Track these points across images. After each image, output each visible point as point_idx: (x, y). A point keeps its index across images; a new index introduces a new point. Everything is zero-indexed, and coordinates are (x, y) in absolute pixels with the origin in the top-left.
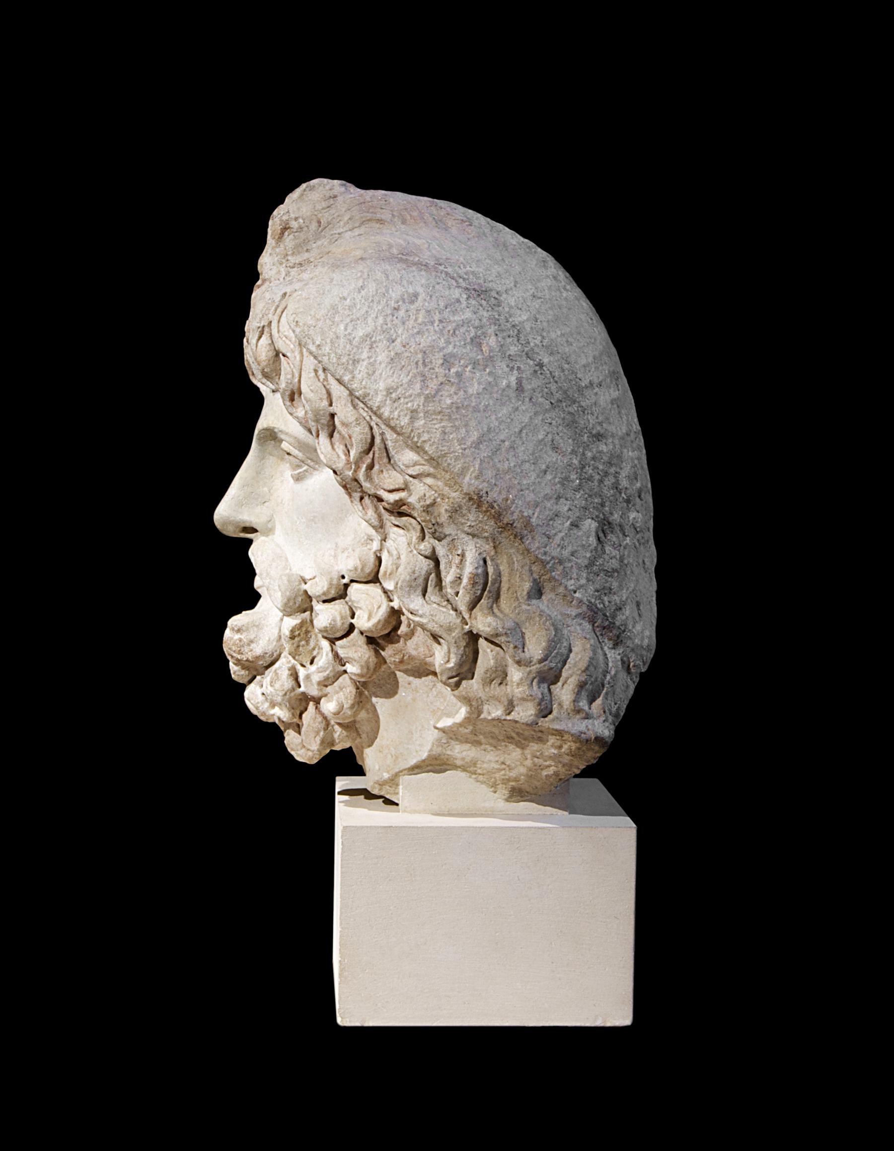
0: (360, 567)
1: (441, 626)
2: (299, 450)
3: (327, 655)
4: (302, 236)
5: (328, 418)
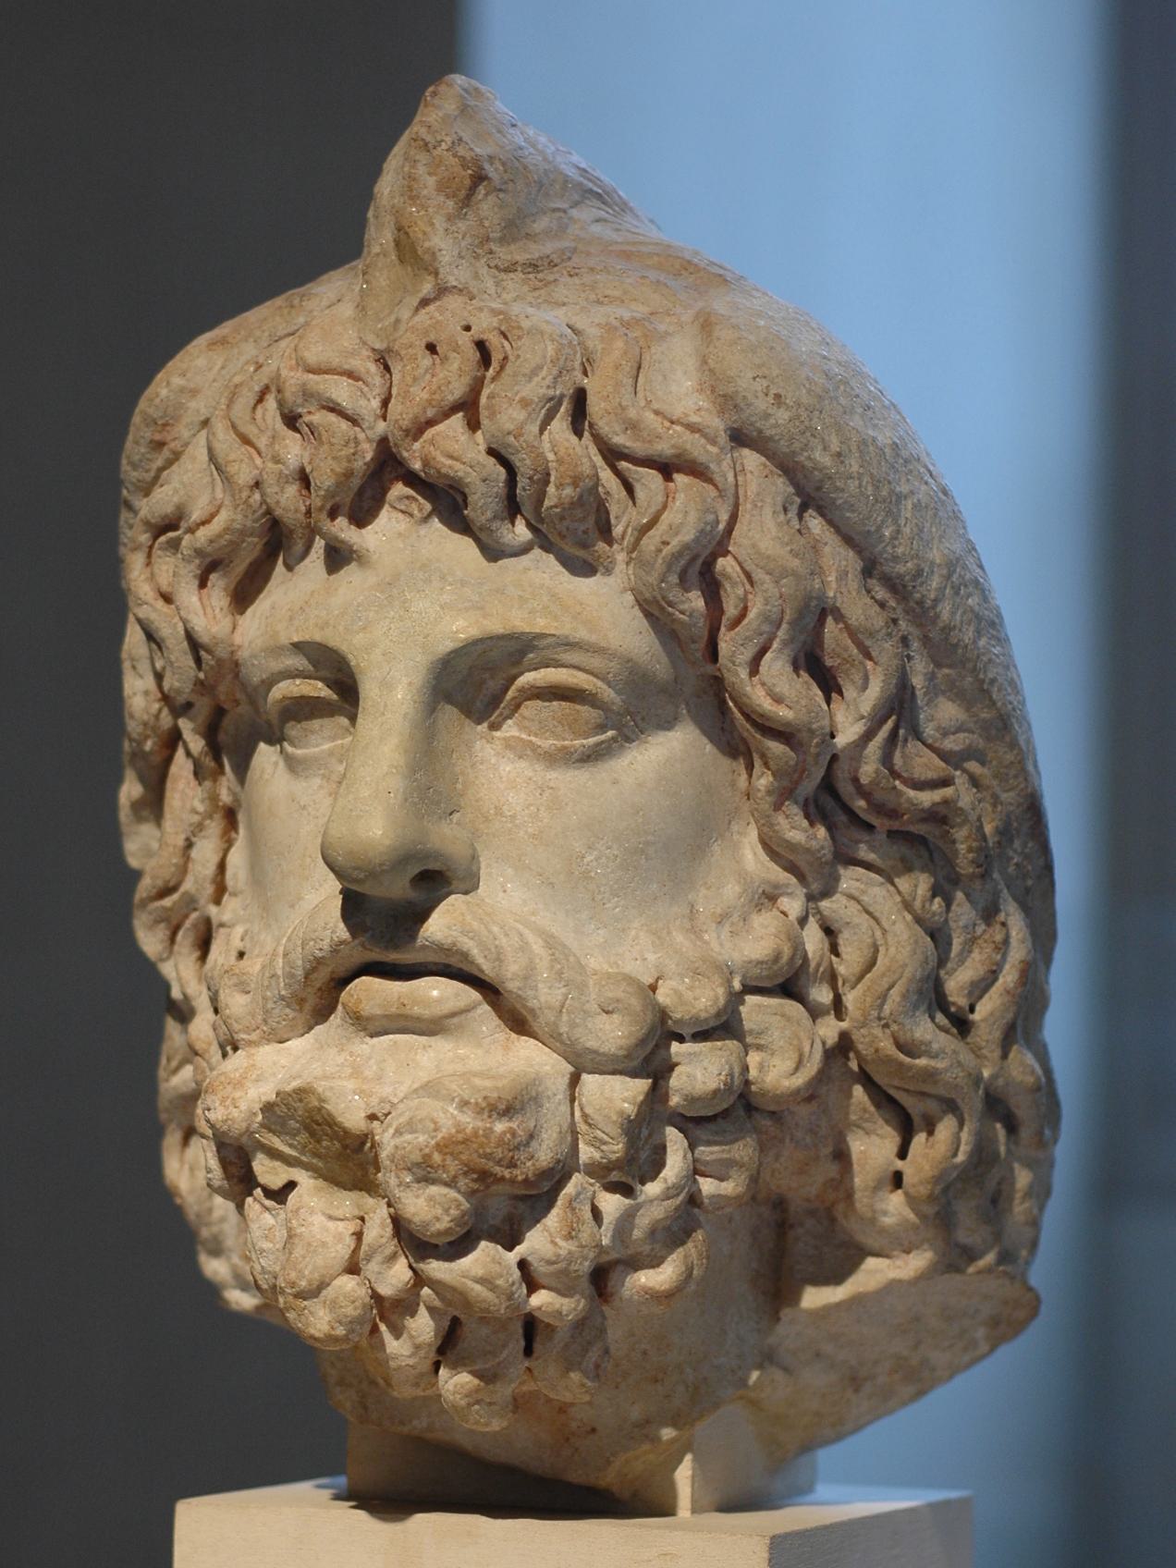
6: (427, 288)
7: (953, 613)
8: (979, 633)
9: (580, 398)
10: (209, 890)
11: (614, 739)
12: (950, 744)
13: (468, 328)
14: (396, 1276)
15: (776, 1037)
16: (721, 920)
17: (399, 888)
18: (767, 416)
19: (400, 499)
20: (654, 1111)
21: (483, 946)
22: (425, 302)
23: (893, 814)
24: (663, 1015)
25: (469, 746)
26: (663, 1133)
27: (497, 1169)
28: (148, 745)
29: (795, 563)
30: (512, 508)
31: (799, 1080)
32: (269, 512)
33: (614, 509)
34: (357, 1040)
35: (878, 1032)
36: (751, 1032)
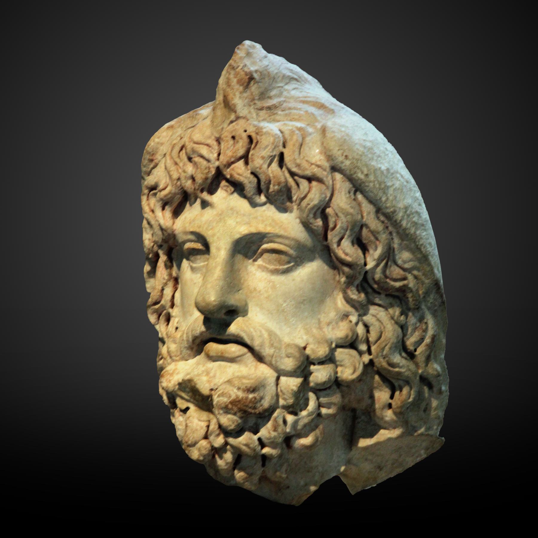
6: (233, 117)
7: (407, 224)
8: (417, 229)
9: (282, 155)
10: (169, 304)
12: (406, 266)
13: (245, 131)
14: (219, 441)
15: (347, 362)
16: (328, 324)
17: (222, 315)
18: (342, 162)
19: (225, 186)
20: (305, 386)
21: (248, 335)
22: (232, 122)
23: (387, 290)
24: (308, 357)
25: (246, 267)
26: (308, 395)
27: (250, 410)
28: (150, 256)
29: (351, 211)
30: (259, 191)
31: (354, 376)
32: (182, 188)
33: (293, 192)
34: (209, 362)
35: (382, 360)
36: (338, 361)
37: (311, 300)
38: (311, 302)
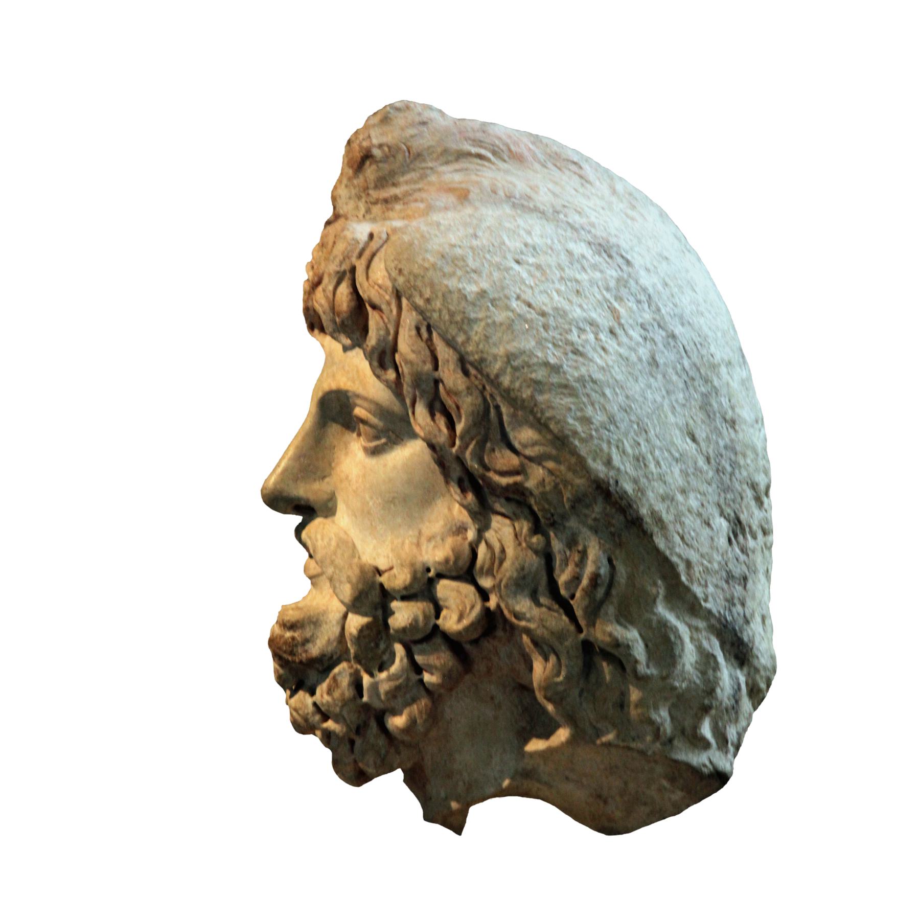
0: (452, 559)
1: (552, 633)
2: (380, 419)
3: (401, 660)
4: (386, 167)
5: (432, 384)
7: (512, 382)
11: (385, 444)
12: (528, 452)
16: (430, 539)
25: (346, 445)
37: (405, 499)
38: (406, 502)
